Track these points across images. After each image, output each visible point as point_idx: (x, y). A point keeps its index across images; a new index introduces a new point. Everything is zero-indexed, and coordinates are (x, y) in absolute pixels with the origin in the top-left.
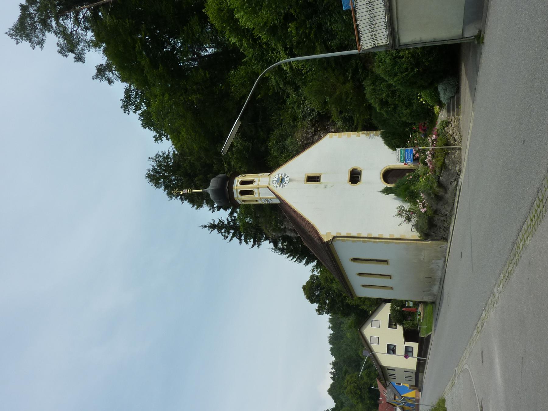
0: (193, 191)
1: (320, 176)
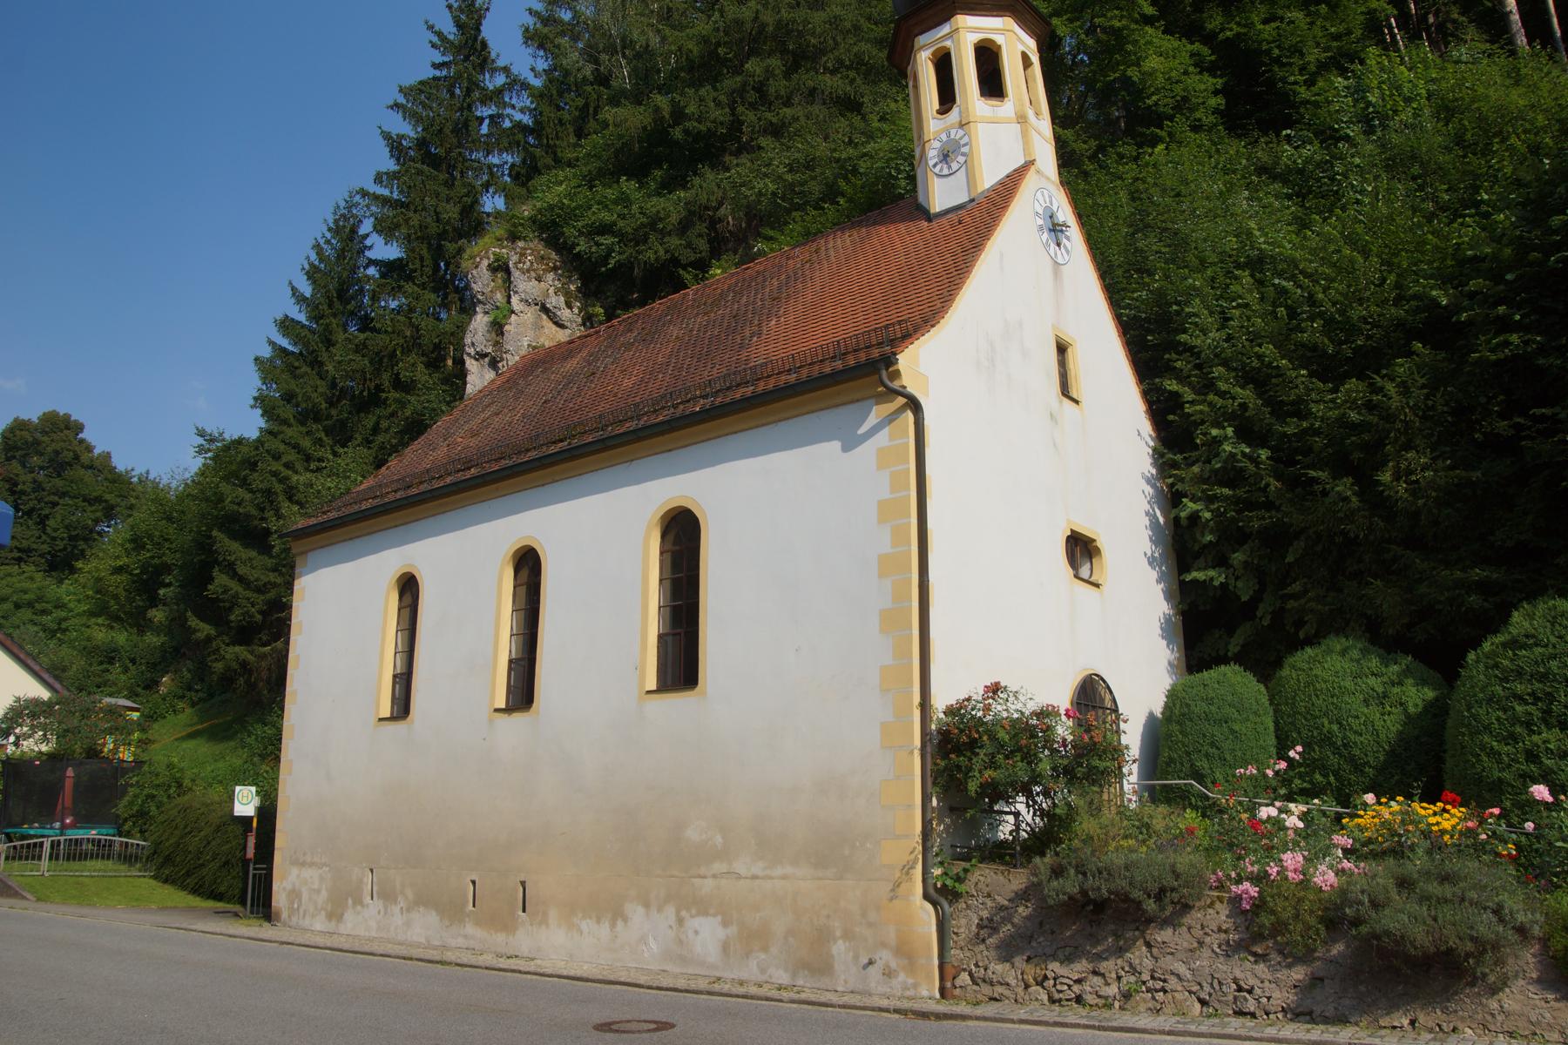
1: (1077, 402)
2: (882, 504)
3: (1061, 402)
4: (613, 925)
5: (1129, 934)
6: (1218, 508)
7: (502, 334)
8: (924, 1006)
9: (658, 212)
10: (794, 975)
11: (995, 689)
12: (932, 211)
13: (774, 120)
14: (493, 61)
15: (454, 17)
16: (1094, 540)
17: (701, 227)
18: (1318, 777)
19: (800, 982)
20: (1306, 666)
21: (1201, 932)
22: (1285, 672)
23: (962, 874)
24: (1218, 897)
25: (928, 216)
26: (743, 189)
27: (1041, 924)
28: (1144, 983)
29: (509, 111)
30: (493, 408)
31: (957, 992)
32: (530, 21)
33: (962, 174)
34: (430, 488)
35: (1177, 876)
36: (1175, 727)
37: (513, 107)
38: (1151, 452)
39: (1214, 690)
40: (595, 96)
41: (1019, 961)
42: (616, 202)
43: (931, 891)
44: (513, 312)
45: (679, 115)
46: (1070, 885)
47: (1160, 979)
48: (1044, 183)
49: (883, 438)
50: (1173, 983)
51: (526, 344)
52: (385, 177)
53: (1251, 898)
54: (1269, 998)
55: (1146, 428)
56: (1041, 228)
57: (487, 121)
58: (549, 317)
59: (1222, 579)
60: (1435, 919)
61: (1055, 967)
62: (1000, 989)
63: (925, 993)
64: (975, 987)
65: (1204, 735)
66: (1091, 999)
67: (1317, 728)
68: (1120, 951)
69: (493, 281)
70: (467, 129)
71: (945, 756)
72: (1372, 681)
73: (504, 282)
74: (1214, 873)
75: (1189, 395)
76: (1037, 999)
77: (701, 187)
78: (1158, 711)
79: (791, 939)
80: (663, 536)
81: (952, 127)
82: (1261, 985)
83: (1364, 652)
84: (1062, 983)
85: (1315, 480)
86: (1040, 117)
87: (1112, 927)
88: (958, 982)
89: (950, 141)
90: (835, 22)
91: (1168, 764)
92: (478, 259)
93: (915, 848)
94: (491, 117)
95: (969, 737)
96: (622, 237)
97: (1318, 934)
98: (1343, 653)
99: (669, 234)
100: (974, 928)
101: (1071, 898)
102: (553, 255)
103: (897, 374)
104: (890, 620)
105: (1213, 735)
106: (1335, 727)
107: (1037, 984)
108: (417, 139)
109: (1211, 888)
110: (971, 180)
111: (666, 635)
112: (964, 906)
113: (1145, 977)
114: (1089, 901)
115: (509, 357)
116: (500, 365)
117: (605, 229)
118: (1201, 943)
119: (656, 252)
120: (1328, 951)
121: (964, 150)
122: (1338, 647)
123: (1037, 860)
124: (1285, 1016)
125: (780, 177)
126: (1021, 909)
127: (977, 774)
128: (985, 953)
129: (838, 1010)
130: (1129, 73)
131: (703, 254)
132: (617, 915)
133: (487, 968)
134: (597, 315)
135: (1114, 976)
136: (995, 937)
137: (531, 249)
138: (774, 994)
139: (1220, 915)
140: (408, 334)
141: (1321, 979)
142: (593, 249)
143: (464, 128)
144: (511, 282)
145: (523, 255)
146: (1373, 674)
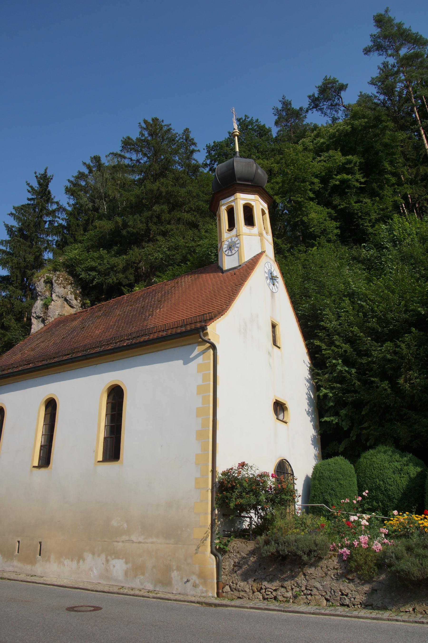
0: (236, 137)
1: (279, 348)
2: (199, 387)
3: (273, 348)
4: (78, 562)
5: (296, 570)
6: (335, 392)
7: (48, 309)
8: (210, 600)
9: (115, 263)
10: (155, 586)
11: (243, 465)
12: (224, 269)
13: (163, 230)
14: (52, 199)
15: (38, 181)
16: (285, 404)
17: (132, 271)
18: (375, 503)
19: (158, 589)
20: (369, 457)
21: (326, 569)
22: (361, 460)
23: (227, 543)
24: (333, 554)
25: (222, 271)
26: (149, 256)
27: (260, 565)
28: (303, 591)
29: (57, 219)
30: (41, 339)
31: (224, 594)
32: (68, 184)
33: (236, 255)
34: (12, 371)
35: (316, 545)
36: (317, 482)
37: (59, 218)
38: (309, 369)
39: (333, 466)
40: (92, 216)
41: (250, 581)
42: (98, 258)
43: (214, 550)
44: (53, 300)
45: (125, 225)
46: (273, 548)
47: (309, 590)
48: (268, 260)
49: (200, 360)
50: (315, 591)
51: (57, 314)
52: (4, 242)
53: (347, 555)
54: (354, 598)
55: (307, 359)
56: (267, 278)
57: (48, 223)
58: (67, 303)
59: (336, 421)
60: (422, 565)
61: (265, 584)
62: (242, 593)
63: (210, 595)
64: (232, 592)
65: (329, 486)
66: (280, 598)
67: (374, 483)
68: (292, 577)
69: (45, 287)
70: (40, 226)
71: (221, 493)
72: (396, 464)
73: (50, 288)
74: (332, 544)
75: (324, 347)
76: (258, 598)
77: (132, 254)
78: (310, 475)
79: (154, 570)
80: (108, 396)
81: (233, 236)
82: (351, 593)
83: (393, 452)
84: (268, 591)
85: (373, 382)
86: (268, 234)
87: (289, 567)
88: (225, 590)
89: (232, 242)
90: (189, 193)
91: (314, 497)
92: (40, 278)
93: (207, 531)
94: (50, 221)
95: (231, 485)
96: (99, 273)
97: (374, 571)
98: (385, 452)
99: (119, 272)
100: (232, 566)
101: (272, 554)
102: (71, 278)
103: (207, 334)
104: (200, 435)
105: (332, 486)
106: (381, 483)
107: (258, 591)
108: (19, 228)
109: (330, 551)
110: (240, 258)
111: (106, 437)
112: (228, 557)
113: (303, 588)
114: (280, 555)
115: (50, 318)
116: (46, 322)
117: (93, 269)
118: (326, 574)
119: (113, 280)
120: (379, 578)
121: (237, 245)
122: (383, 450)
123: (259, 537)
124: (361, 606)
125: (164, 252)
126: (251, 558)
127: (234, 500)
128: (236, 577)
129: (173, 602)
130: (304, 219)
131: (132, 281)
132: (80, 557)
133: (21, 581)
134: (87, 304)
135: (290, 588)
136: (241, 570)
137: (62, 275)
138: (146, 594)
139: (334, 562)
140: (9, 306)
141: (376, 590)
142: (87, 277)
143: (38, 225)
144: (53, 288)
145: (58, 277)
146: (397, 461)
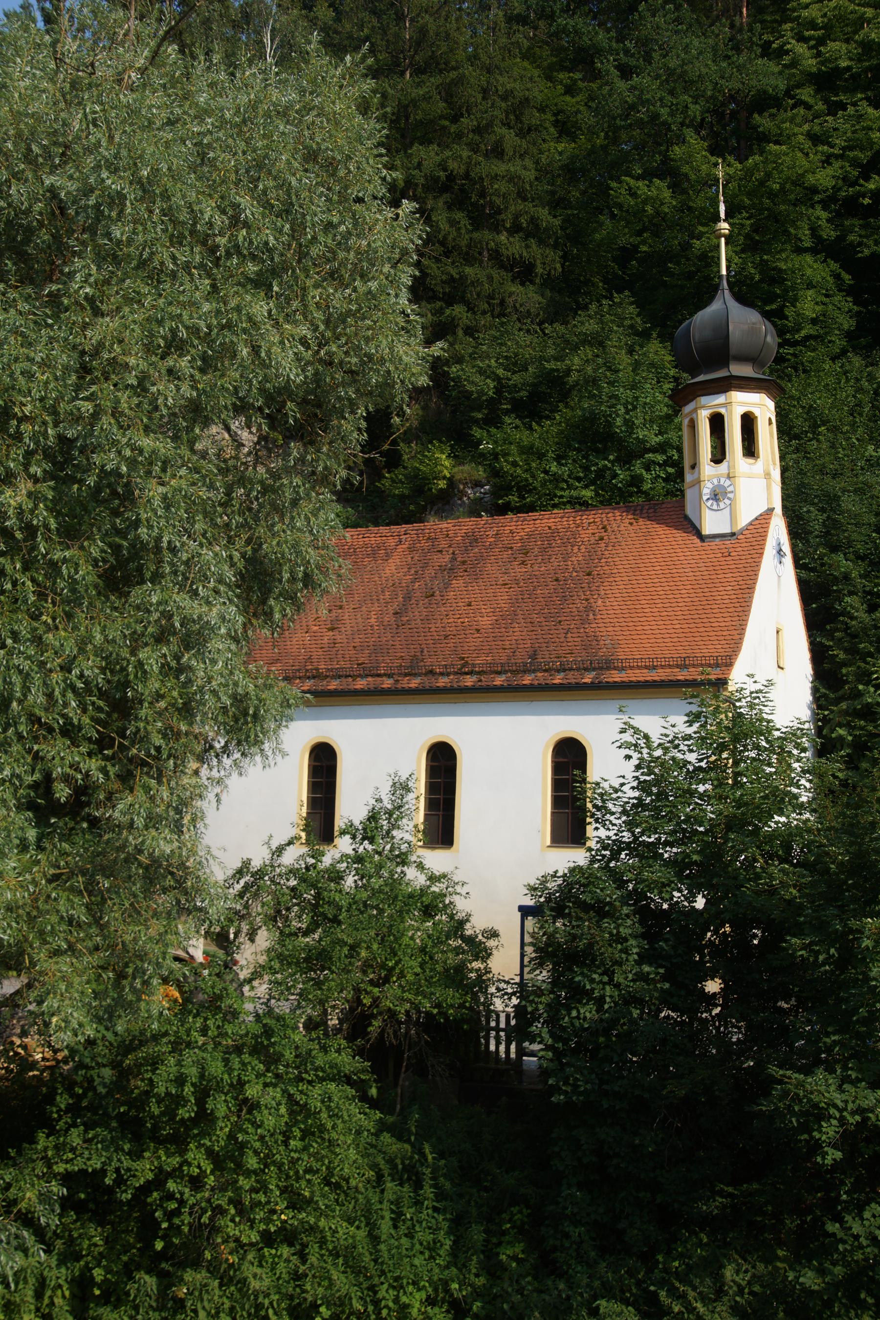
81: (722, 475)
